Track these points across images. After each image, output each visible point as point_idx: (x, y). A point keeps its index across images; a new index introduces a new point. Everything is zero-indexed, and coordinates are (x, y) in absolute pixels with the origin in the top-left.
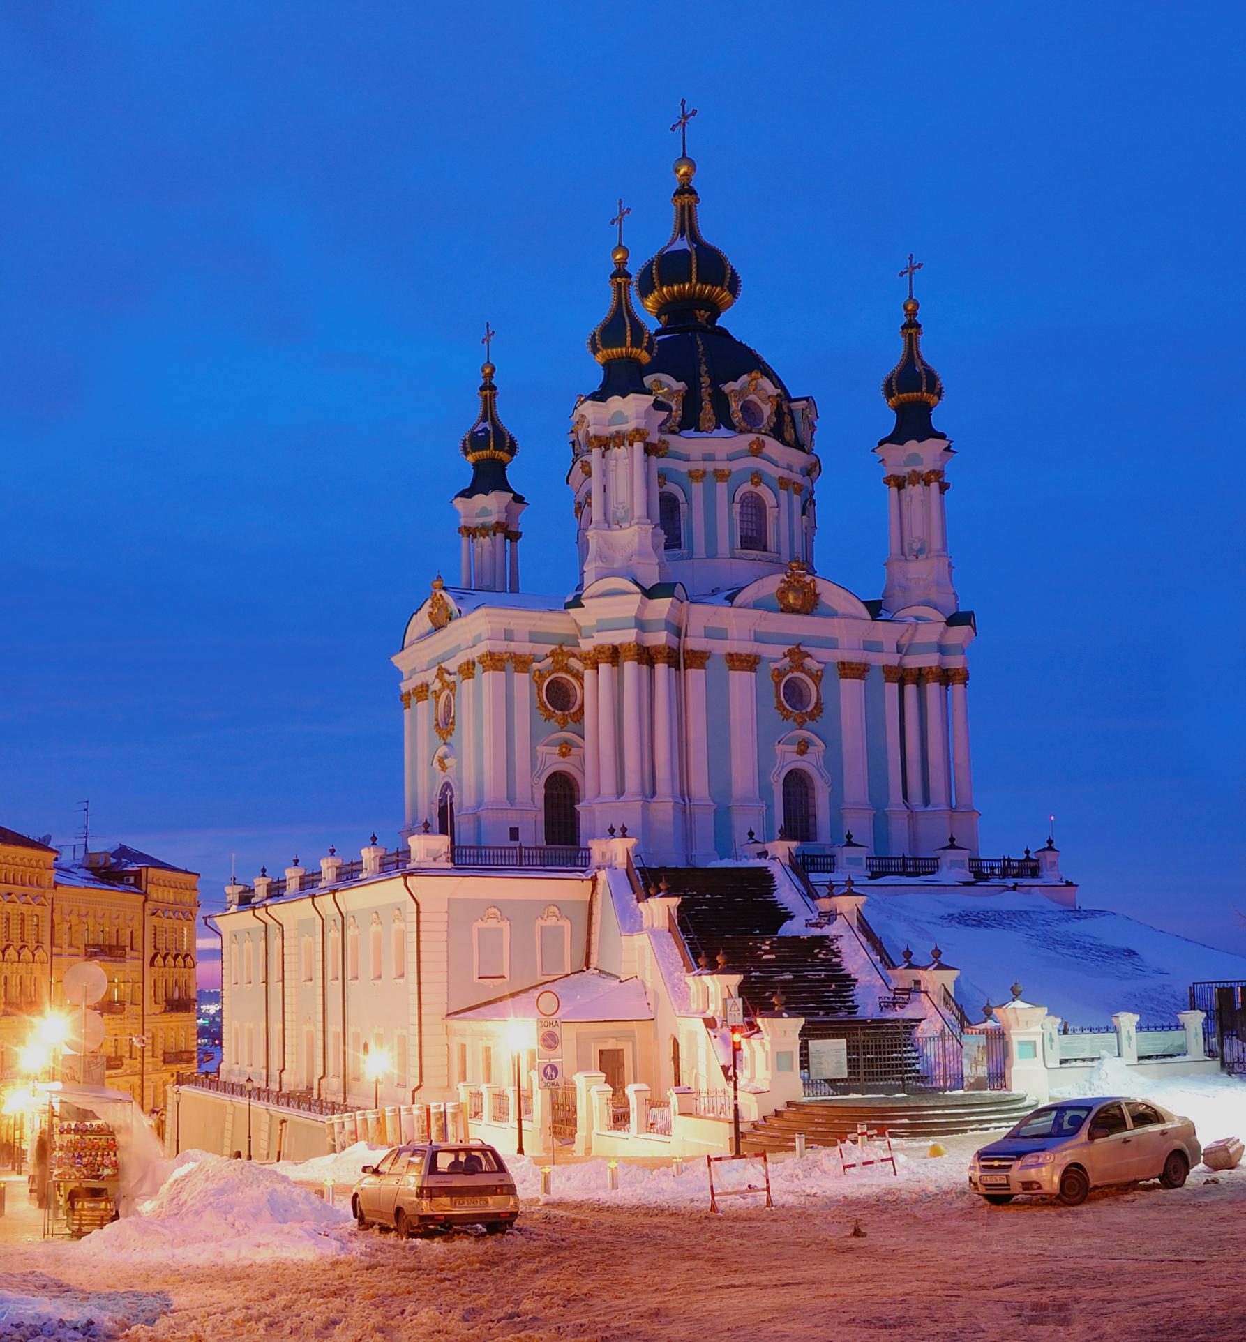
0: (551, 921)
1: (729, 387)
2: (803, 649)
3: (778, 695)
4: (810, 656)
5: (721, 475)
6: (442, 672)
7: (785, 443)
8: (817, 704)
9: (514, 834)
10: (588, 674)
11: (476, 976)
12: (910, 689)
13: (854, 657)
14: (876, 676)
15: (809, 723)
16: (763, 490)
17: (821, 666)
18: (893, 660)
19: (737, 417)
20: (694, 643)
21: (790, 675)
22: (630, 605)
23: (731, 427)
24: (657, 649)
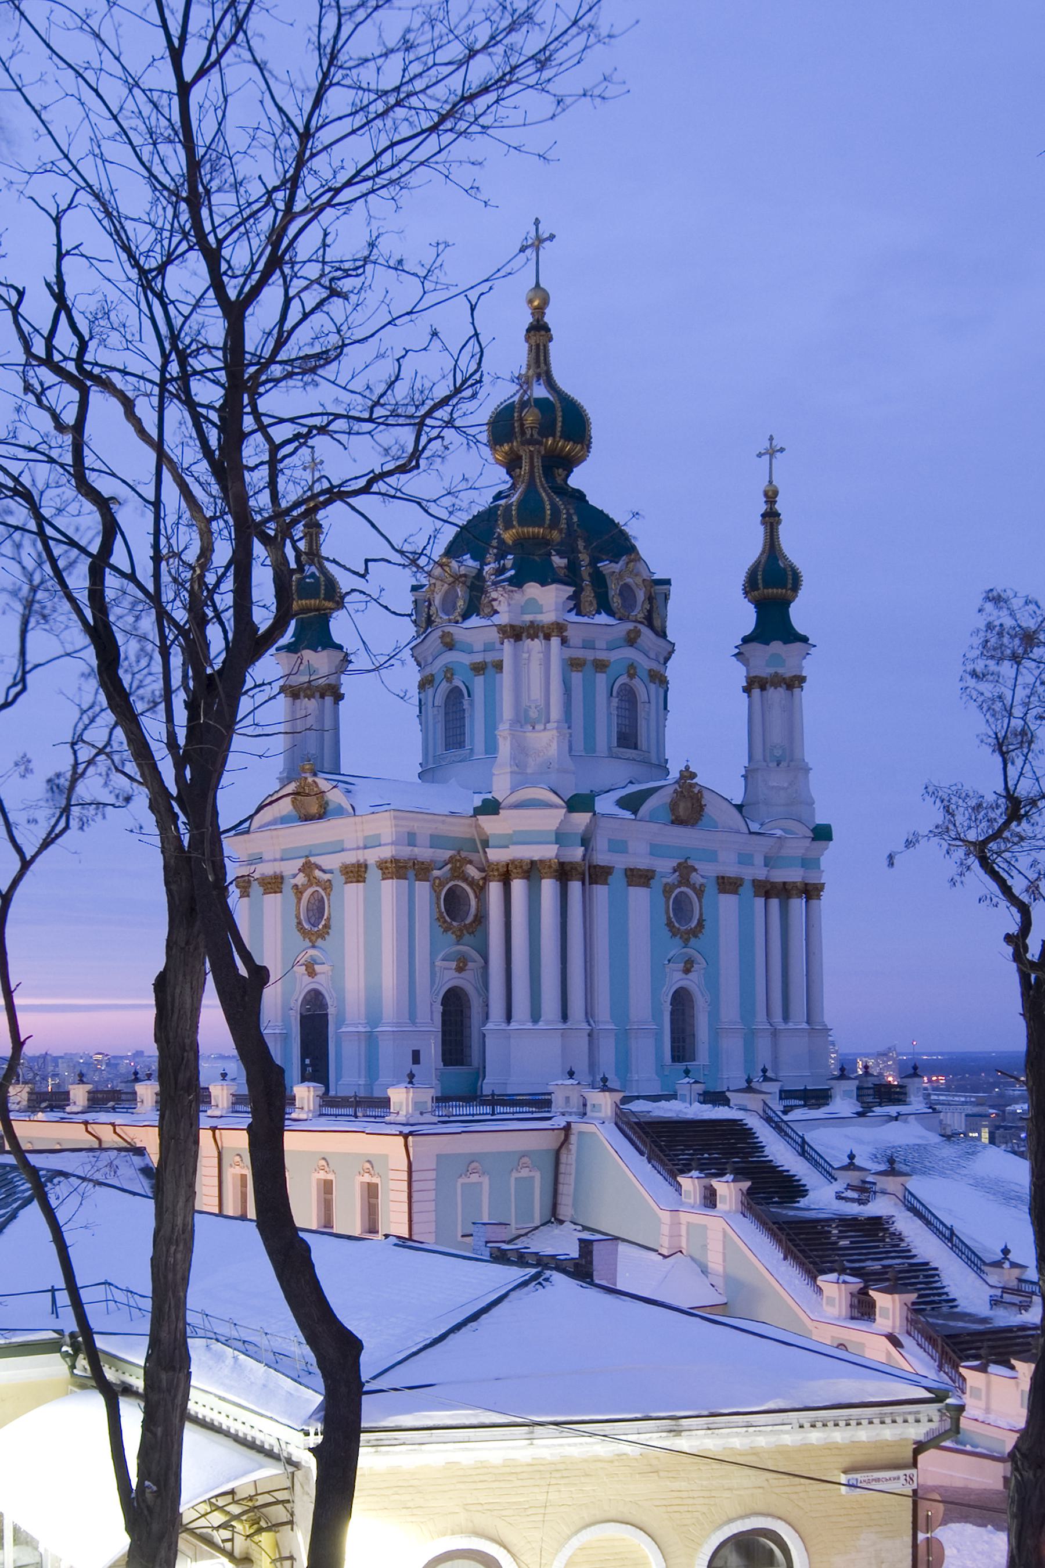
0: (525, 1173)
1: (606, 567)
2: (690, 862)
3: (667, 912)
4: (695, 870)
5: (601, 666)
6: (308, 868)
8: (699, 920)
9: (416, 1057)
10: (495, 889)
11: (460, 1239)
13: (731, 871)
14: (747, 889)
16: (637, 683)
18: (761, 873)
19: (616, 602)
20: (602, 857)
22: (552, 819)
23: (611, 613)
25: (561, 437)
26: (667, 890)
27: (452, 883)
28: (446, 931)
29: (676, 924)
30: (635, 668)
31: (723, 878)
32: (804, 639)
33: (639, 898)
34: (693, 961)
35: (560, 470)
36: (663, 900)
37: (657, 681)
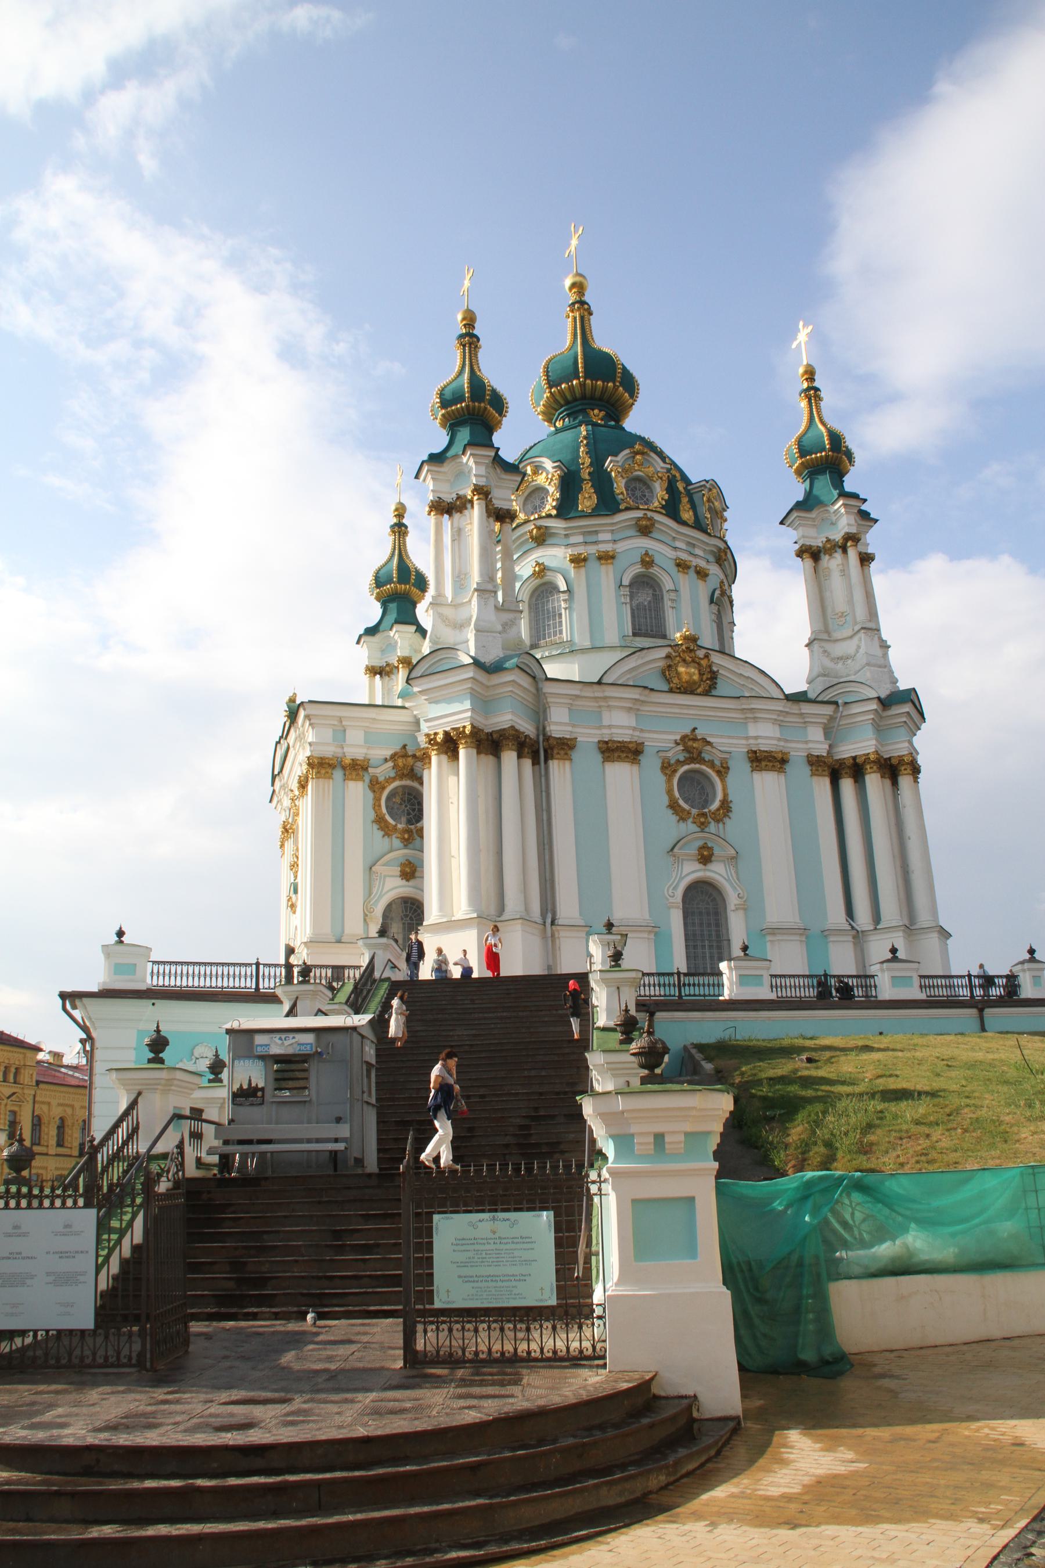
2: (700, 733)
3: (670, 792)
4: (709, 743)
7: (684, 523)
12: (847, 786)
15: (712, 827)
21: (686, 767)
24: (502, 733)
25: (586, 377)
26: (668, 768)
27: (397, 783)
28: (387, 834)
29: (686, 806)
30: (650, 557)
31: (755, 752)
32: (855, 496)
33: (620, 773)
34: (711, 849)
35: (596, 411)
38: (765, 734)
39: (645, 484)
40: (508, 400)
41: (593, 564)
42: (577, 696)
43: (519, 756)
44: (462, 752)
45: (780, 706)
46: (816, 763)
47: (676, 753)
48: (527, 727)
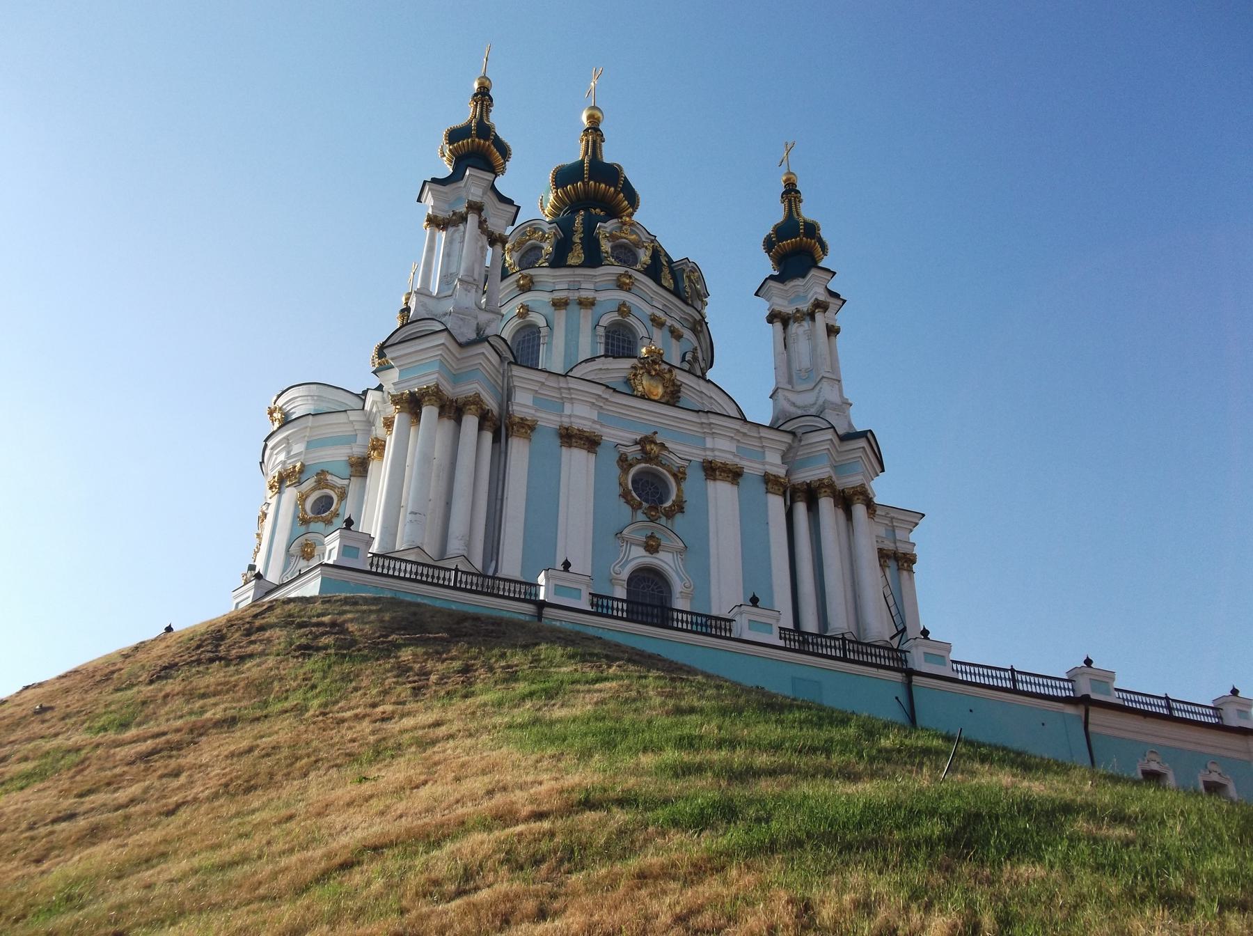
4: (666, 448)
17: (686, 464)
25: (590, 179)
26: (624, 463)
36: (617, 471)
37: (666, 329)
38: (723, 449)
39: (630, 251)
40: (513, 151)
41: (573, 308)
42: (543, 384)
43: (481, 428)
44: (424, 410)
45: (737, 425)
46: (770, 481)
47: (633, 451)
48: (491, 403)
